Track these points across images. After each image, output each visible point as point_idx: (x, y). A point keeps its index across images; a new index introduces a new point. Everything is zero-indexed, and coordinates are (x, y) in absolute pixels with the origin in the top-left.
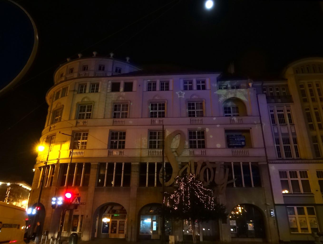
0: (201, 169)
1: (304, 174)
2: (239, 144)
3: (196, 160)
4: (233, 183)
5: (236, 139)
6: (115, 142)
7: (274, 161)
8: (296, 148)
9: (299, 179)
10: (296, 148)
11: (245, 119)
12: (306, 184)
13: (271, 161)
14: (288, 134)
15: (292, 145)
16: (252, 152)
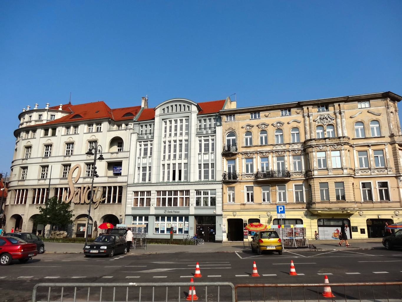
0: (87, 191)
1: (149, 193)
2: (119, 172)
3: (85, 185)
4: (105, 199)
5: (117, 168)
6: (43, 173)
7: (130, 185)
8: (150, 174)
9: (145, 197)
10: (150, 174)
11: (121, 155)
12: (149, 200)
13: (130, 185)
14: (146, 164)
15: (148, 172)
16: (119, 179)
